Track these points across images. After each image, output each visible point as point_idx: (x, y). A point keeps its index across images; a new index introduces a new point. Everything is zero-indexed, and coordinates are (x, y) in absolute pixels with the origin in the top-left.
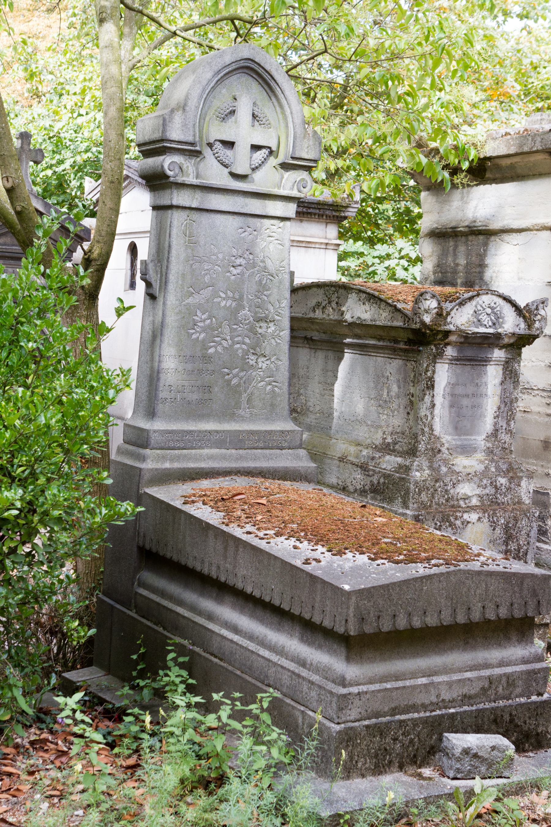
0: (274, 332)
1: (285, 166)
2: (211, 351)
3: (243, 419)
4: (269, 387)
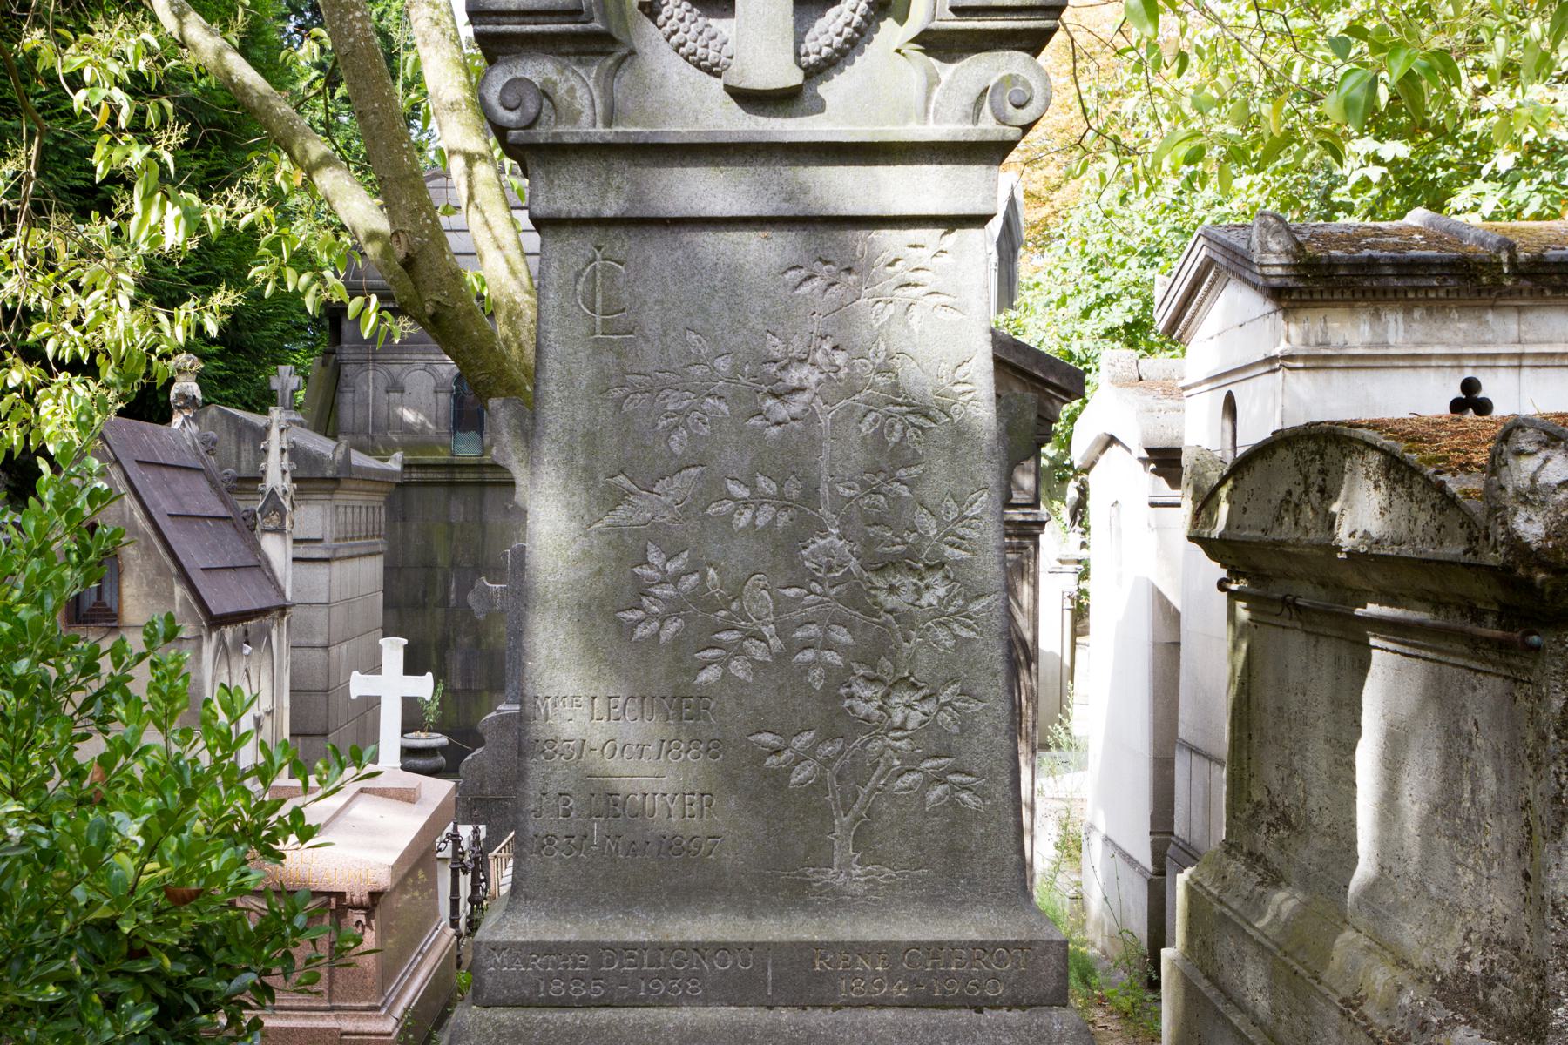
0: (945, 601)
1: (937, 44)
2: (709, 675)
3: (837, 901)
4: (939, 790)
